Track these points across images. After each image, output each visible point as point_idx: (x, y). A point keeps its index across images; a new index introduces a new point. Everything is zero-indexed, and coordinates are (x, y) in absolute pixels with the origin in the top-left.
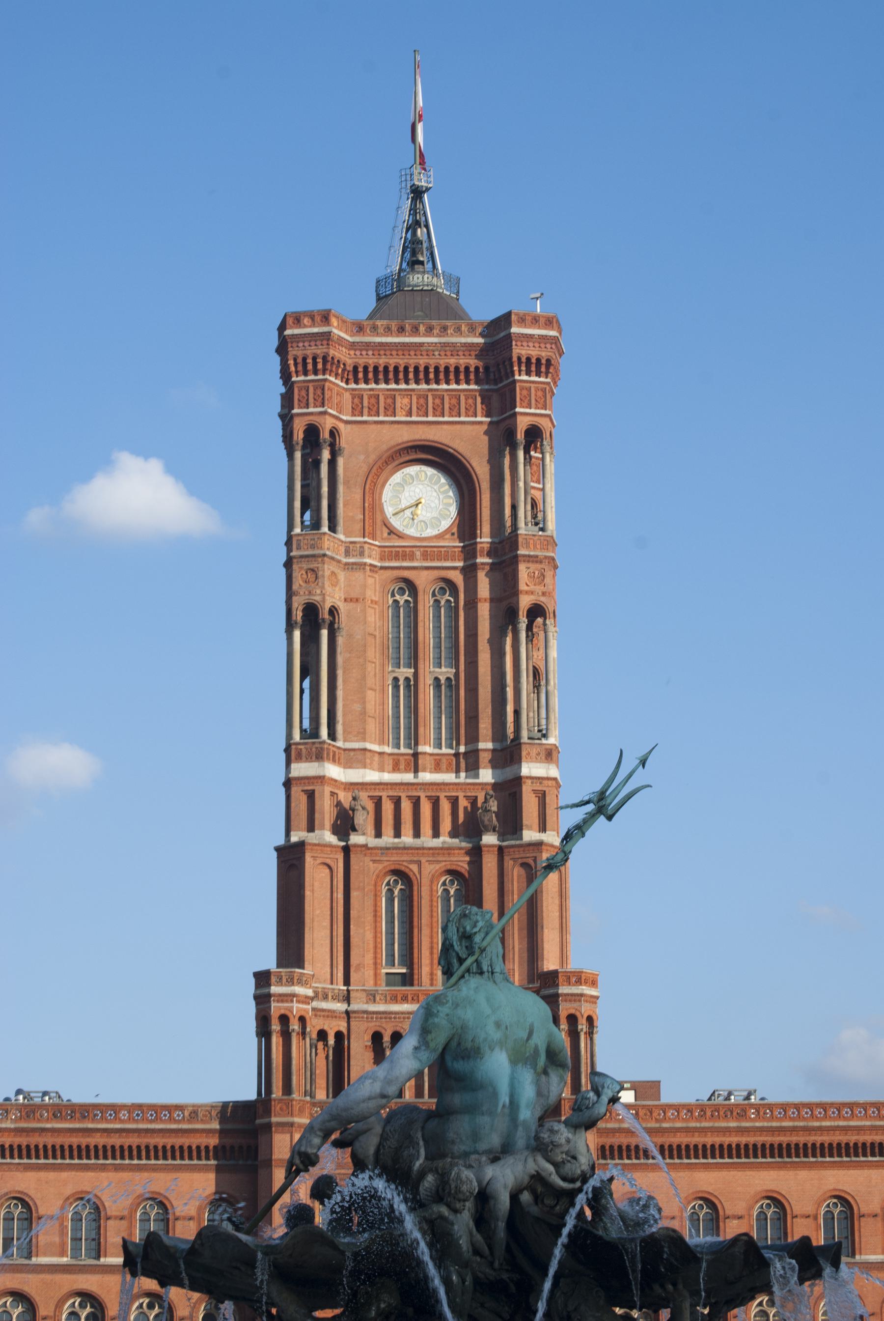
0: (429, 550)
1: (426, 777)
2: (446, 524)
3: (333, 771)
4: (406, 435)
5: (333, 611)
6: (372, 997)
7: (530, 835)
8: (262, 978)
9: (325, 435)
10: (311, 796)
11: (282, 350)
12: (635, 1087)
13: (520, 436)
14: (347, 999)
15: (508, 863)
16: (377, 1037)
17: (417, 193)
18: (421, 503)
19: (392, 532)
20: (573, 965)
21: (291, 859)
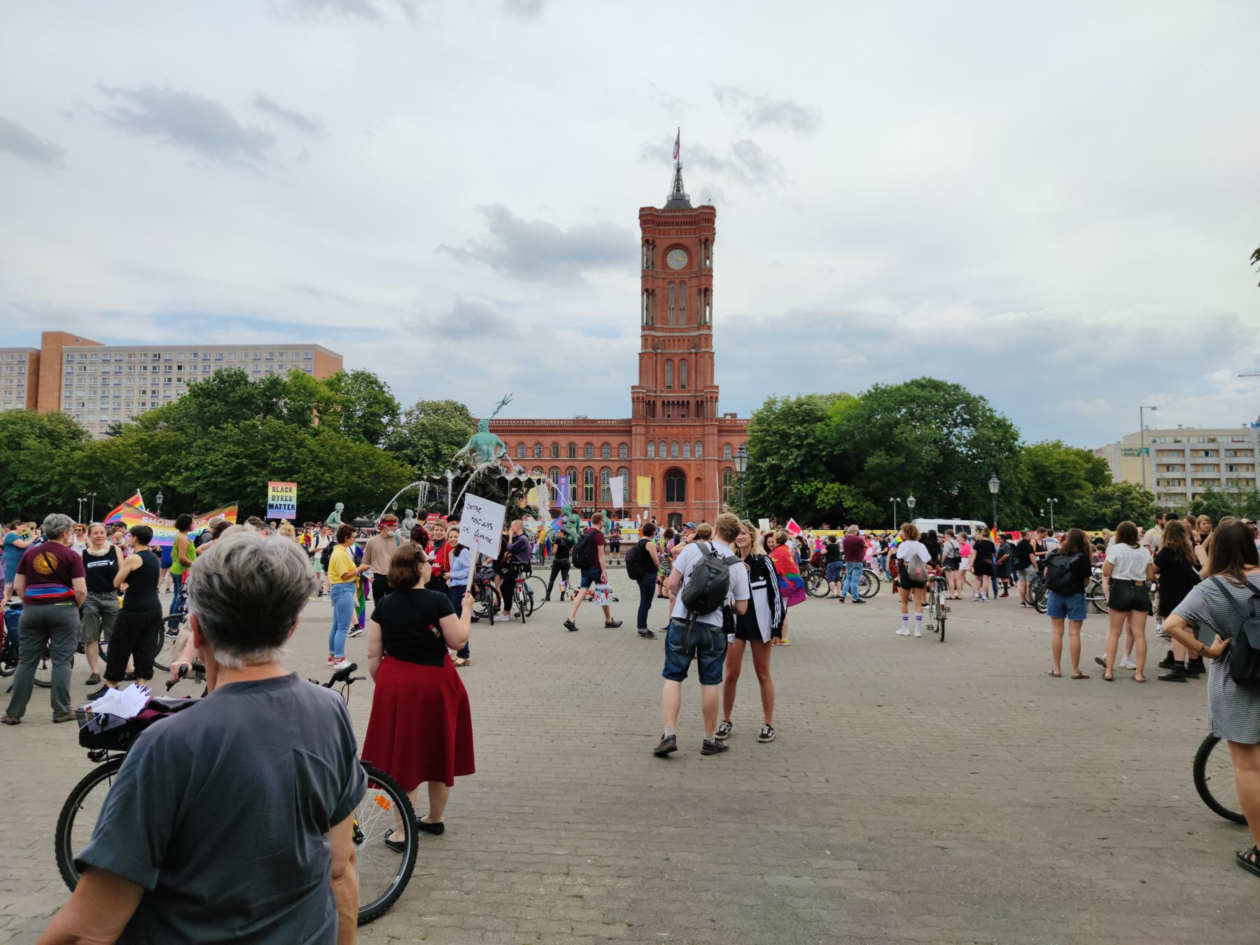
0: (679, 273)
3: (653, 333)
7: (704, 350)
8: (633, 387)
17: (678, 170)
18: (677, 260)
21: (642, 355)
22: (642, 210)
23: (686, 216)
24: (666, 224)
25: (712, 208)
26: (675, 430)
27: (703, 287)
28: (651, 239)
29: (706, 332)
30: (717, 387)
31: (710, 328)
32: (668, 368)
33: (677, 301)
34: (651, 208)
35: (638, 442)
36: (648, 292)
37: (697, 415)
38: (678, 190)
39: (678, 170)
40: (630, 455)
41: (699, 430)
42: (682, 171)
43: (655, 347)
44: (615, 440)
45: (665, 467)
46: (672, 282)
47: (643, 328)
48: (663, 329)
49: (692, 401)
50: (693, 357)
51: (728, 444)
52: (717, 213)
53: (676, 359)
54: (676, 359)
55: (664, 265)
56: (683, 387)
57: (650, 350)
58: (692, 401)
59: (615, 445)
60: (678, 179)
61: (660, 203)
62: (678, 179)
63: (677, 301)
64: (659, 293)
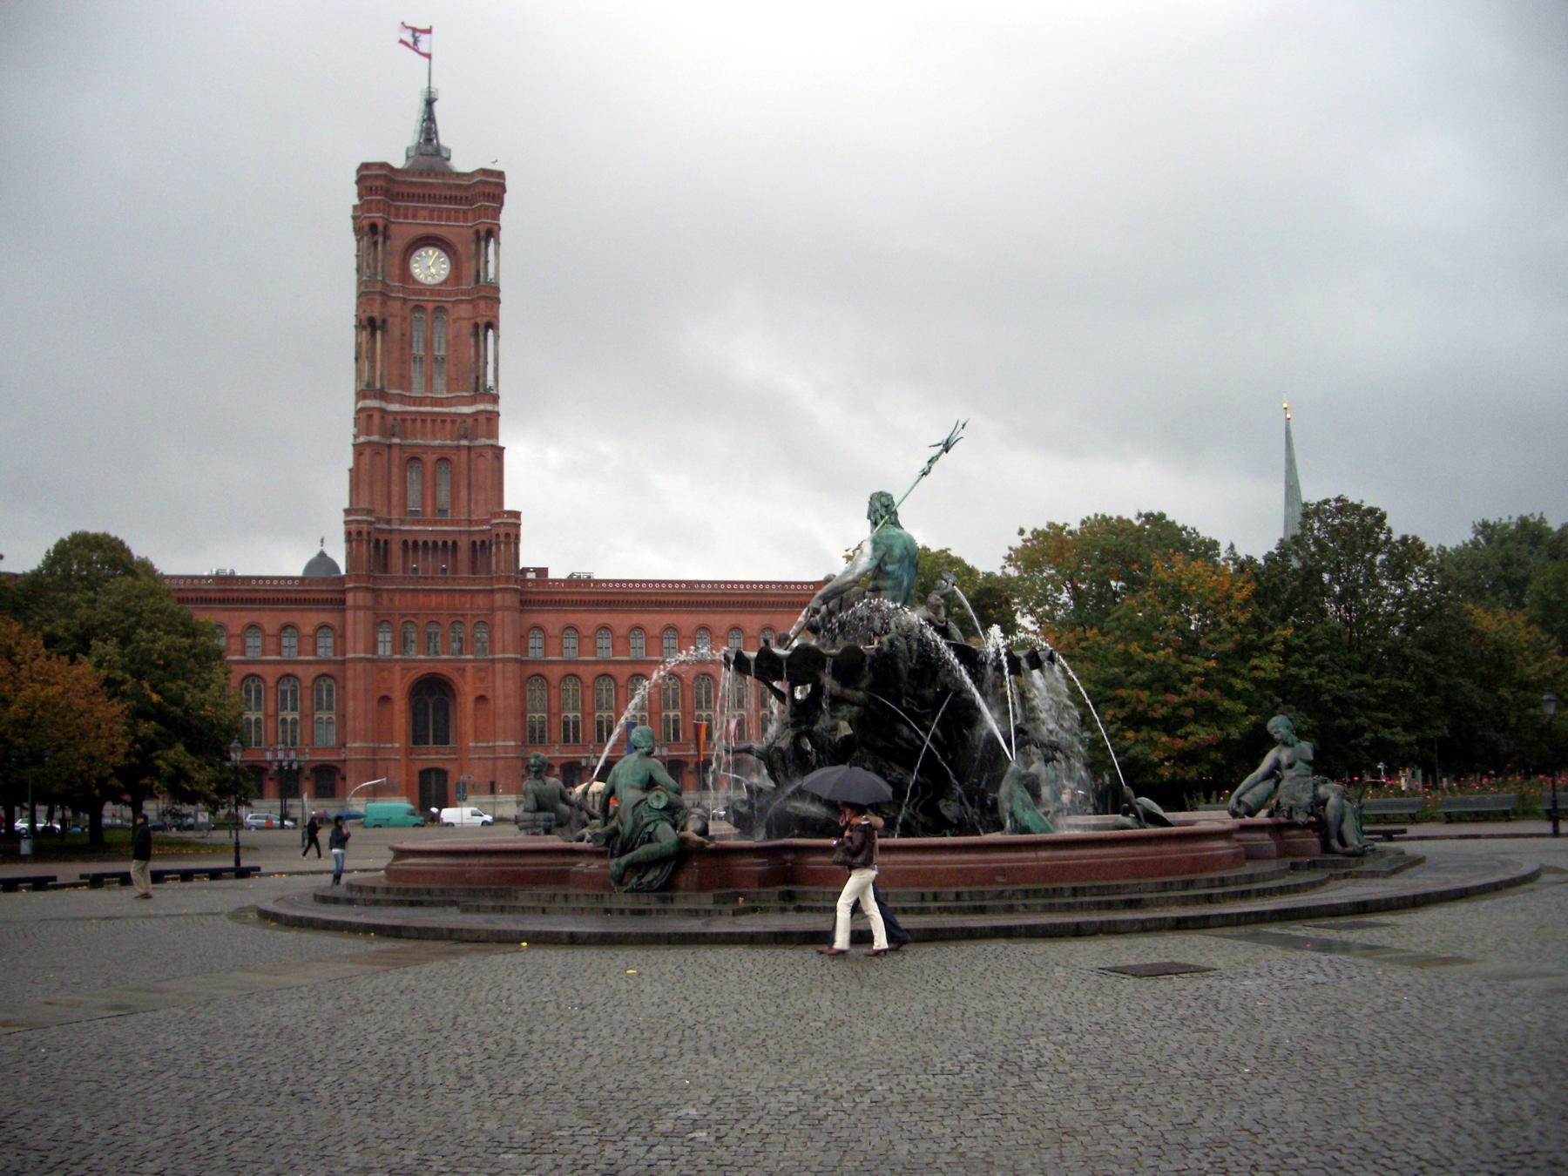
1: (428, 409)
2: (442, 278)
3: (384, 405)
4: (422, 231)
5: (384, 321)
6: (402, 522)
7: (483, 441)
9: (380, 228)
10: (370, 417)
11: (358, 182)
12: (536, 570)
13: (483, 234)
14: (389, 522)
15: (473, 455)
16: (405, 543)
17: (430, 103)
18: (430, 267)
19: (416, 282)
20: (508, 506)
22: (365, 166)
23: (449, 187)
24: (412, 197)
25: (501, 175)
26: (434, 600)
27: (482, 321)
28: (380, 223)
29: (489, 407)
30: (517, 515)
31: (495, 399)
32: (413, 477)
33: (429, 345)
34: (383, 165)
35: (356, 622)
36: (369, 325)
37: (474, 570)
38: (429, 140)
39: (430, 103)
40: (340, 648)
41: (481, 600)
42: (437, 107)
43: (388, 432)
44: (309, 620)
45: (413, 675)
46: (419, 308)
47: (361, 395)
48: (403, 400)
49: (464, 543)
50: (464, 454)
51: (539, 628)
52: (509, 184)
53: (430, 459)
54: (430, 459)
55: (406, 275)
56: (443, 512)
57: (375, 438)
58: (464, 543)
59: (308, 629)
60: (429, 118)
61: (396, 153)
62: (429, 118)
63: (429, 345)
64: (395, 326)
